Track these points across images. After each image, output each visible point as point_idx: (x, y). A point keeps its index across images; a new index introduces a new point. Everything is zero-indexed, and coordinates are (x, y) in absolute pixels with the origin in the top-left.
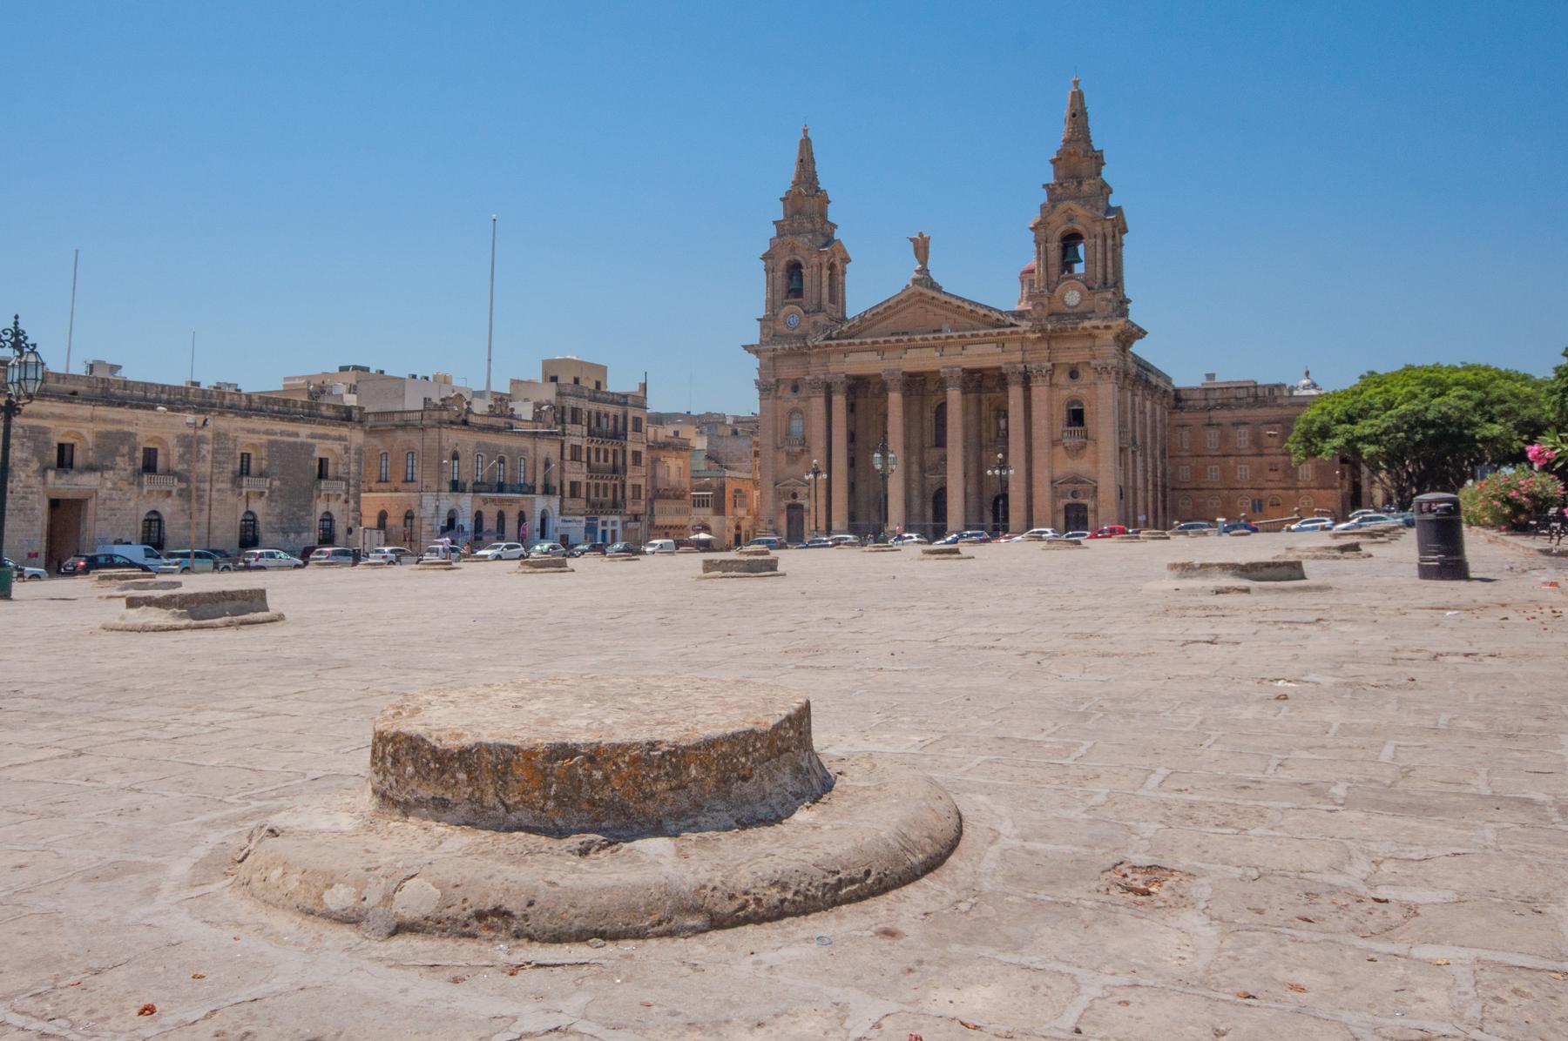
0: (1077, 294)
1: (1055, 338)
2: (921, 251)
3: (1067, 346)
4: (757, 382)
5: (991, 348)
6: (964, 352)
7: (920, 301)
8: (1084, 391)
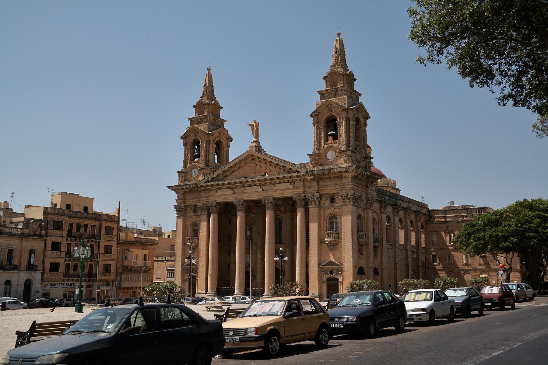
1: (321, 179)
3: (328, 183)
4: (175, 207)
5: (288, 185)
6: (275, 188)
7: (253, 159)
8: (337, 210)
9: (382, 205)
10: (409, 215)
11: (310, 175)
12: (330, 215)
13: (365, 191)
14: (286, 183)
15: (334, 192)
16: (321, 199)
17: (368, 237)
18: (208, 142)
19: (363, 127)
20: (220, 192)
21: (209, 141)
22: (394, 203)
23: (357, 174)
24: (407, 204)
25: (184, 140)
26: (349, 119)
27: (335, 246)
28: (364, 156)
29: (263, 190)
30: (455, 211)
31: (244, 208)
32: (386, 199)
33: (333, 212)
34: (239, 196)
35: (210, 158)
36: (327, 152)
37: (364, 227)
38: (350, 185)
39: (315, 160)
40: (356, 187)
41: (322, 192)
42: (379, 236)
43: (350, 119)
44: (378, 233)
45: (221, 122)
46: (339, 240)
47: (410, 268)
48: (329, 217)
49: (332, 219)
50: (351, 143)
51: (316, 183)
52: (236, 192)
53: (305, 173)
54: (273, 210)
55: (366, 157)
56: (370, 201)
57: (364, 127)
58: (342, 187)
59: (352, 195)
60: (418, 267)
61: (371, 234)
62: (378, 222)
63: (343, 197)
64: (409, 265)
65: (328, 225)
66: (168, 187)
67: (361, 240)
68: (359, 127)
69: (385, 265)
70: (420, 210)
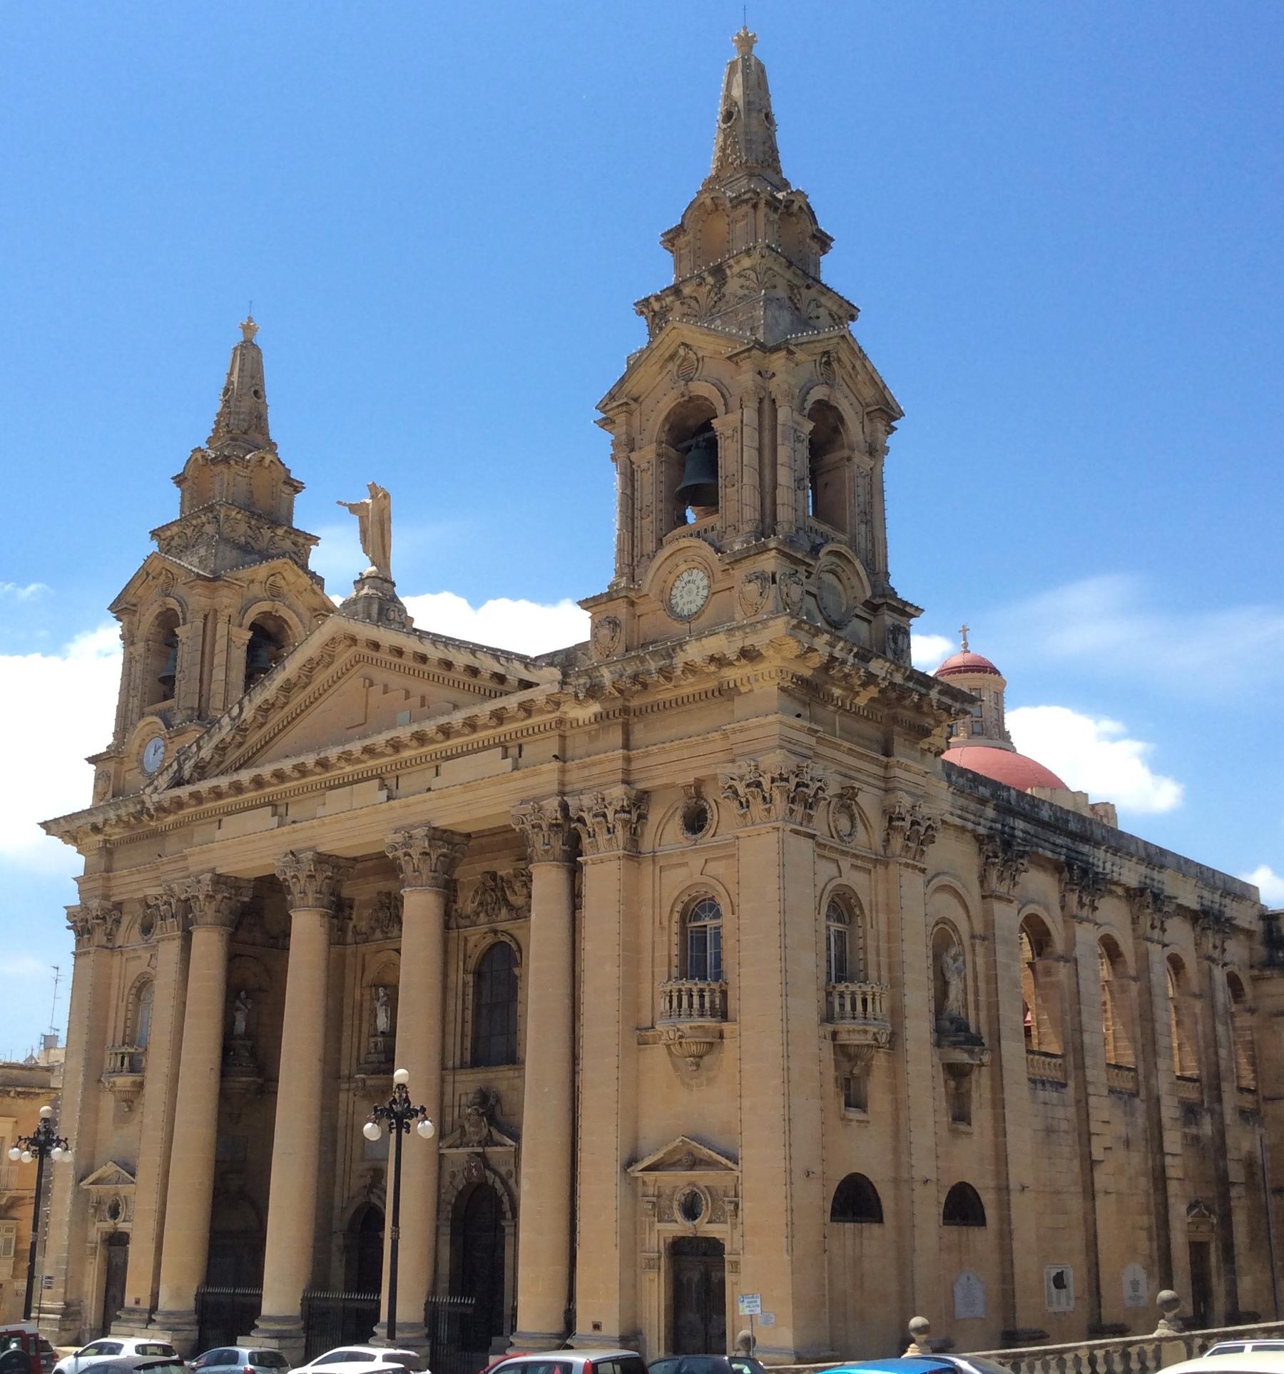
0: (699, 577)
1: (641, 712)
2: (373, 531)
4: (71, 914)
6: (436, 783)
7: (358, 660)
8: (717, 868)
9: (988, 857)
10: (1158, 924)
11: (581, 696)
12: (686, 898)
13: (880, 772)
15: (700, 773)
16: (642, 817)
17: (897, 1013)
18: (210, 617)
19: (862, 461)
21: (216, 611)
22: (1063, 858)
23: (811, 672)
24: (1142, 869)
25: (125, 618)
26: (774, 401)
27: (706, 1058)
28: (869, 594)
29: (389, 798)
31: (320, 892)
32: (1013, 828)
33: (697, 878)
35: (213, 686)
36: (672, 577)
37: (872, 957)
38: (771, 723)
39: (614, 623)
40: (812, 741)
41: (647, 779)
42: (983, 1014)
43: (779, 397)
44: (971, 998)
45: (295, 544)
46: (726, 1027)
47: (1173, 1187)
48: (679, 907)
49: (697, 917)
50: (780, 517)
51: (616, 737)
53: (555, 688)
54: (437, 893)
55: (881, 601)
56: (907, 824)
57: (866, 458)
58: (733, 739)
59: (782, 779)
60: (1224, 1183)
61: (918, 999)
62: (973, 946)
63: (736, 793)
64: (1171, 1172)
65: (675, 951)
67: (845, 1026)
68: (842, 459)
69: (1019, 1172)
70: (1217, 906)
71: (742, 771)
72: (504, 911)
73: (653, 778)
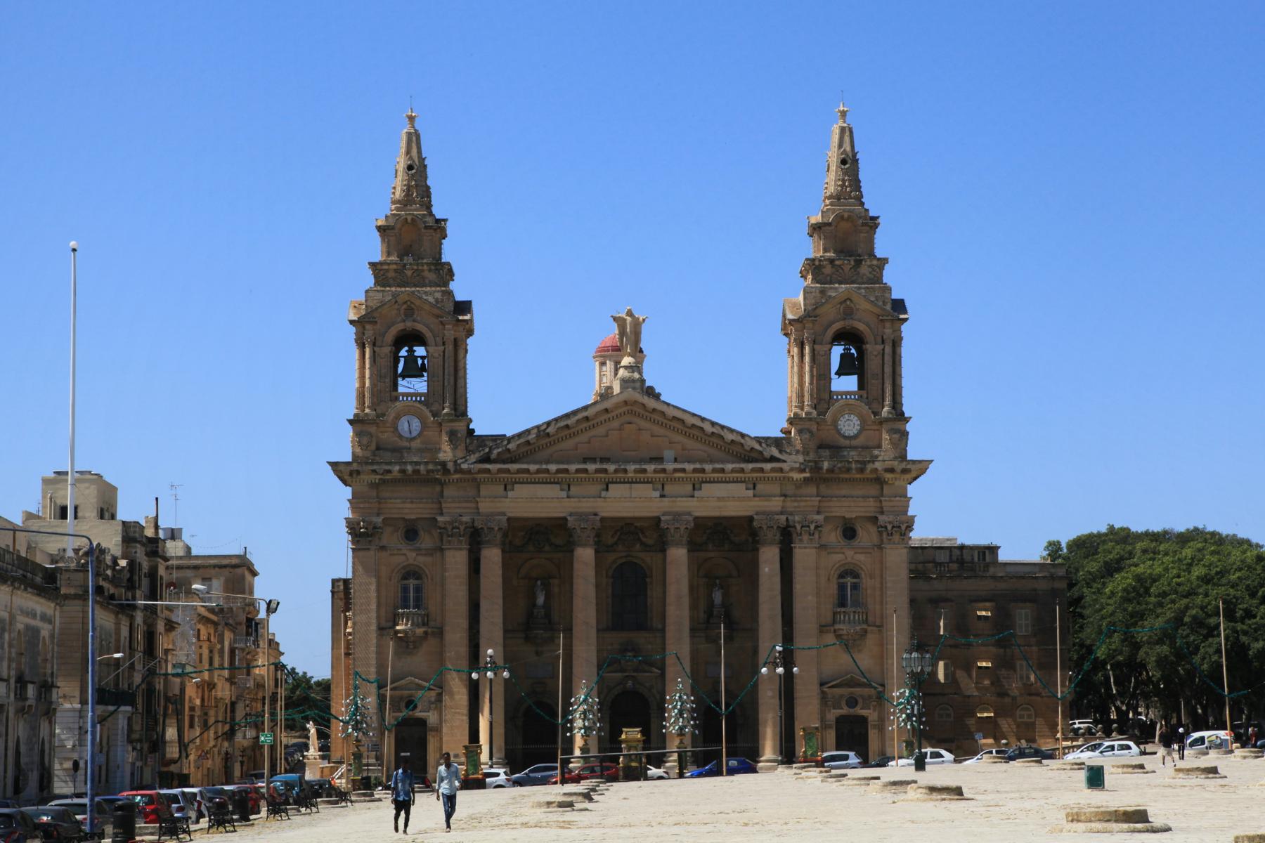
3: (844, 492)
5: (739, 490)
14: (733, 482)
20: (521, 491)
30: (920, 551)
34: (586, 506)
52: (571, 493)
66: (330, 463)
71: (890, 520)
72: (638, 546)
73: (832, 512)
